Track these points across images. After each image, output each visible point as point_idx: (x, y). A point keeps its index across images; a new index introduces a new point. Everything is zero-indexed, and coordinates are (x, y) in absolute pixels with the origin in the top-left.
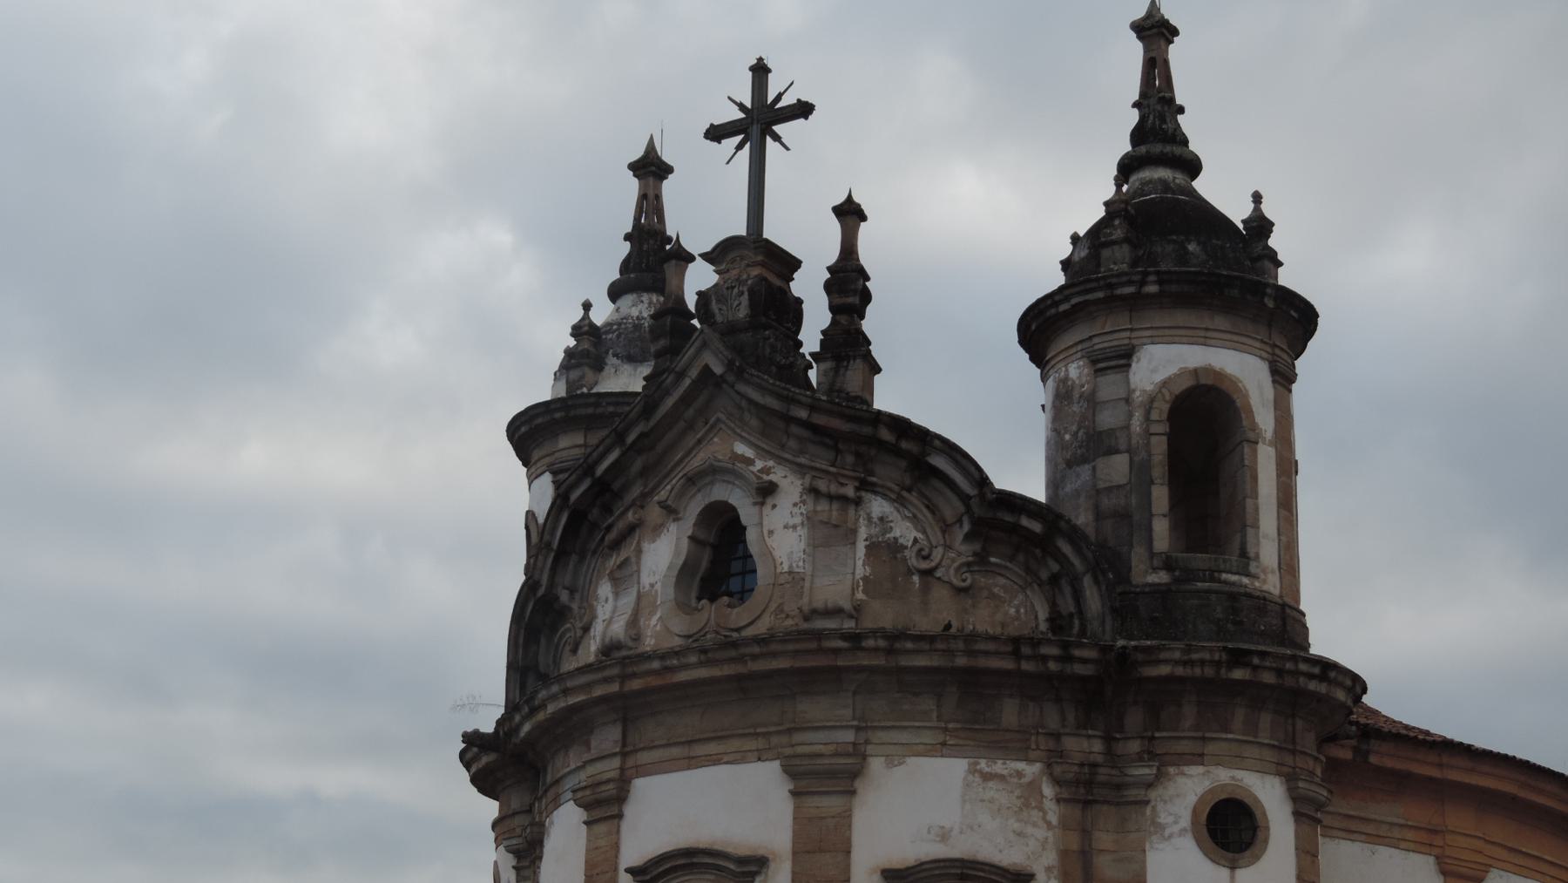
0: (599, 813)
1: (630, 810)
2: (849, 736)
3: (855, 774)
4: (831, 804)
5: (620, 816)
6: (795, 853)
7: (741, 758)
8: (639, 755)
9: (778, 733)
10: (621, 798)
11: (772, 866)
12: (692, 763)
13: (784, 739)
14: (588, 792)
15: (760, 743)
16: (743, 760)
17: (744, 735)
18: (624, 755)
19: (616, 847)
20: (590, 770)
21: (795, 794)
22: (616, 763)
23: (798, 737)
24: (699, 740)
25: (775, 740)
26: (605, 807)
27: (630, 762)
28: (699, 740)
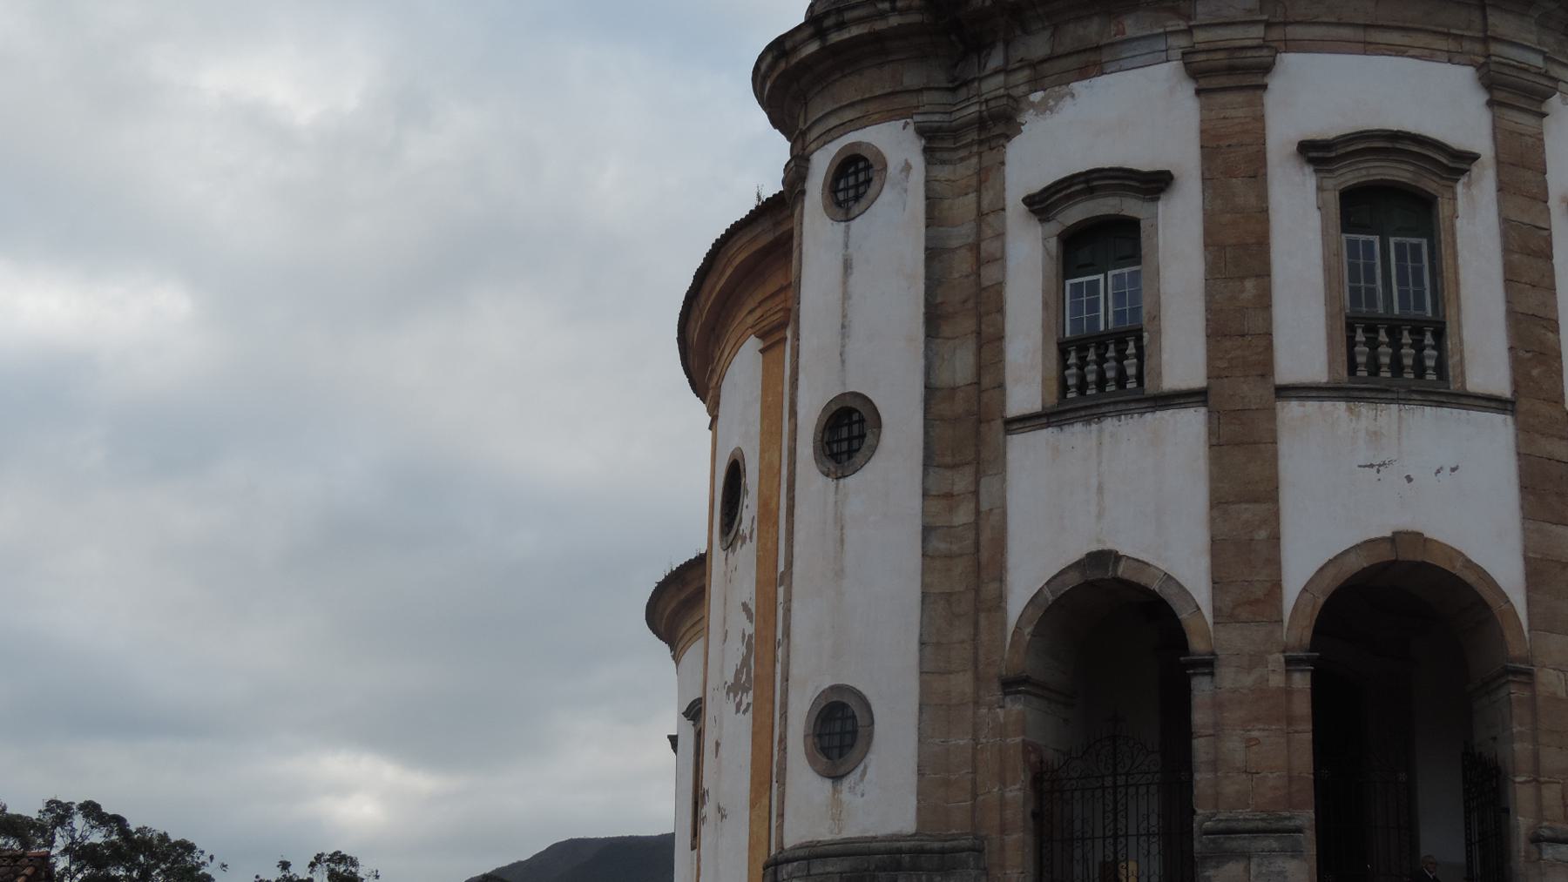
0: (1215, 82)
1: (1276, 83)
2: (1538, 61)
3: (1545, 96)
4: (1526, 121)
5: (1264, 87)
6: (1499, 162)
7: (1429, 55)
8: (1289, 29)
9: (1472, 39)
10: (1267, 69)
11: (1475, 169)
12: (1368, 48)
13: (1478, 48)
14: (1220, 55)
15: (1451, 45)
16: (1430, 58)
17: (1435, 33)
18: (1268, 25)
19: (1260, 119)
20: (1200, 36)
21: (1491, 103)
22: (1257, 32)
23: (1495, 48)
24: (1382, 27)
25: (1467, 46)
26: (1232, 77)
27: (1276, 34)
28: (1382, 27)
